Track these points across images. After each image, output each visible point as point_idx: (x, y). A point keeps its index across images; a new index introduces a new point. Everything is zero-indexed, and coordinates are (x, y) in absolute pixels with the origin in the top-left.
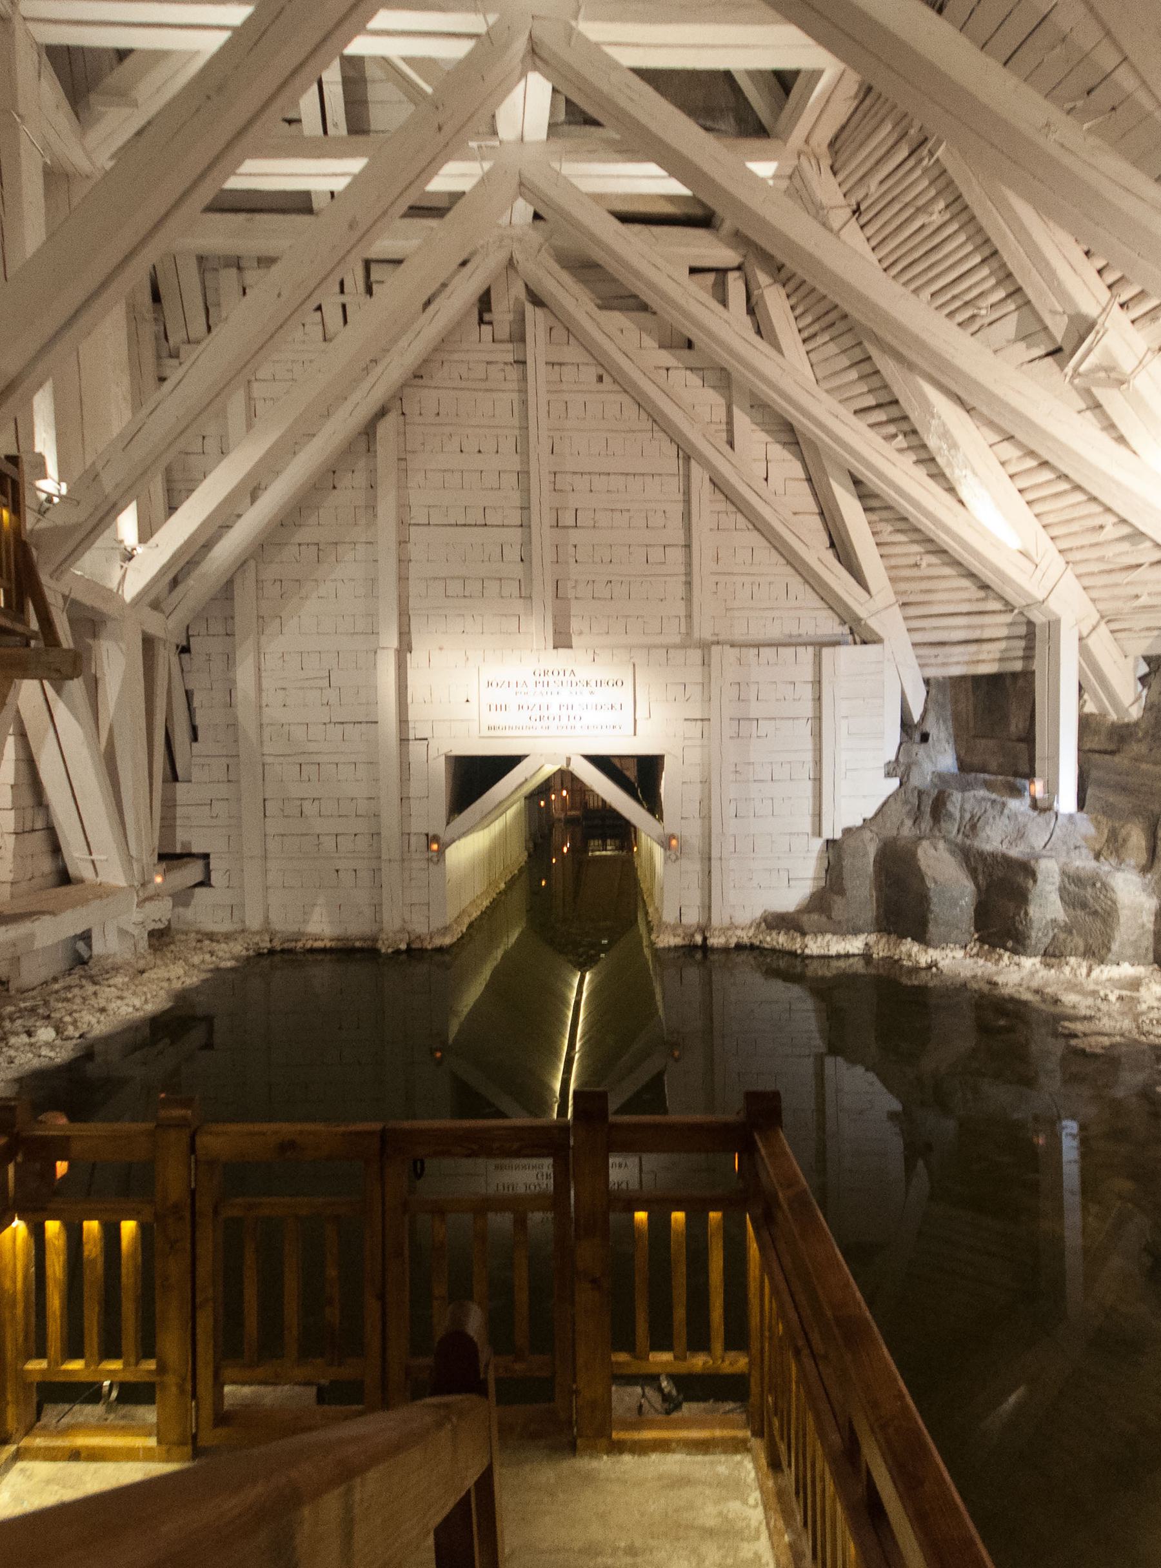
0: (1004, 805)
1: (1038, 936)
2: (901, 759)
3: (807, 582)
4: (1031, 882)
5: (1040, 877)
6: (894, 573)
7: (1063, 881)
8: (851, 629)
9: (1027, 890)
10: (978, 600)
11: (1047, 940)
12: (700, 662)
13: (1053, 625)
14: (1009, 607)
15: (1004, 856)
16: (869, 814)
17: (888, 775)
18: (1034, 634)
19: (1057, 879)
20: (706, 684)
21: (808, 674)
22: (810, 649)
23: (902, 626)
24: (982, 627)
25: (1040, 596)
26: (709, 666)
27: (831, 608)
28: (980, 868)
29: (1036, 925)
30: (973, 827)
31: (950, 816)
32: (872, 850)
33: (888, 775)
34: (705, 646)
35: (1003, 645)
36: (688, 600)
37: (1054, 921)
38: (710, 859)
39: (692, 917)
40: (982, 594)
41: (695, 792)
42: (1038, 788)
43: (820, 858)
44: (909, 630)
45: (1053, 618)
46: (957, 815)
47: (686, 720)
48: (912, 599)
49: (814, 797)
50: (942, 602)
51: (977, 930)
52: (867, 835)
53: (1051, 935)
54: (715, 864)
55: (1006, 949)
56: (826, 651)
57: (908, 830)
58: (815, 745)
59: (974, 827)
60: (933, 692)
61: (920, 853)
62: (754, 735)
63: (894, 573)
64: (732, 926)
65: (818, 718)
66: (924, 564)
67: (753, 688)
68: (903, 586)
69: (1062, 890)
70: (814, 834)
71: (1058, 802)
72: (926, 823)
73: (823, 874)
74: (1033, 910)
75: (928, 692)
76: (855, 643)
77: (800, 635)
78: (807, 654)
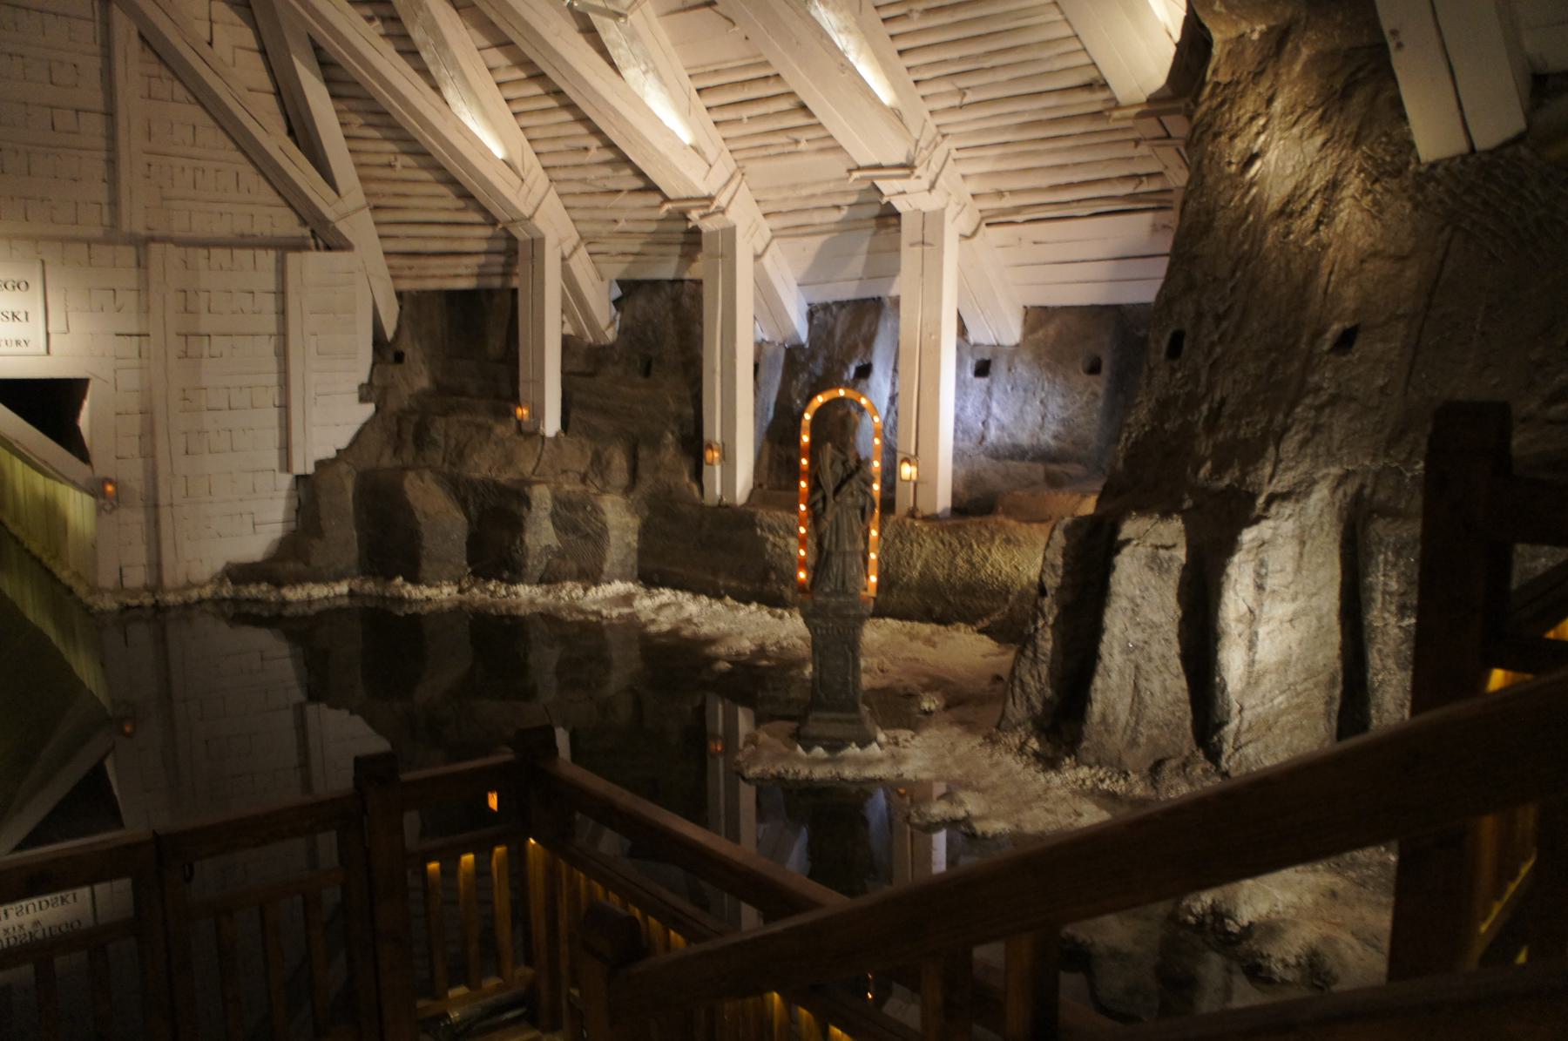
0: (490, 429)
1: (534, 564)
2: (375, 382)
3: (262, 173)
4: (525, 509)
5: (534, 503)
6: (366, 171)
7: (554, 506)
8: (313, 232)
9: (524, 518)
10: (458, 210)
11: (542, 567)
12: (133, 261)
13: (537, 243)
14: (493, 222)
15: (495, 483)
16: (343, 443)
17: (363, 399)
18: (516, 252)
19: (549, 504)
20: (143, 288)
21: (270, 282)
22: (272, 254)
23: (373, 232)
24: (462, 238)
25: (527, 212)
26: (146, 268)
27: (291, 206)
28: (470, 498)
29: (531, 553)
30: (461, 455)
31: (434, 443)
32: (349, 484)
33: (363, 399)
34: (142, 243)
35: (482, 259)
36: (112, 181)
37: (549, 547)
38: (156, 506)
39: (137, 577)
40: (461, 204)
41: (134, 424)
42: (522, 412)
43: (289, 497)
44: (381, 237)
45: (536, 236)
46: (442, 443)
47: (117, 335)
48: (383, 202)
49: (280, 426)
50: (417, 208)
51: (470, 563)
52: (343, 468)
53: (545, 560)
54: (164, 512)
55: (502, 580)
56: (293, 258)
57: (387, 461)
58: (279, 365)
59: (461, 455)
60: (406, 307)
61: (407, 484)
62: (206, 353)
63: (366, 171)
64: (190, 585)
65: (283, 334)
66: (398, 165)
67: (203, 296)
68: (374, 187)
69: (554, 516)
70: (281, 470)
71: (544, 426)
72: (408, 455)
73: (293, 515)
74: (529, 539)
75: (401, 307)
76: (317, 248)
77: (254, 236)
78: (268, 258)
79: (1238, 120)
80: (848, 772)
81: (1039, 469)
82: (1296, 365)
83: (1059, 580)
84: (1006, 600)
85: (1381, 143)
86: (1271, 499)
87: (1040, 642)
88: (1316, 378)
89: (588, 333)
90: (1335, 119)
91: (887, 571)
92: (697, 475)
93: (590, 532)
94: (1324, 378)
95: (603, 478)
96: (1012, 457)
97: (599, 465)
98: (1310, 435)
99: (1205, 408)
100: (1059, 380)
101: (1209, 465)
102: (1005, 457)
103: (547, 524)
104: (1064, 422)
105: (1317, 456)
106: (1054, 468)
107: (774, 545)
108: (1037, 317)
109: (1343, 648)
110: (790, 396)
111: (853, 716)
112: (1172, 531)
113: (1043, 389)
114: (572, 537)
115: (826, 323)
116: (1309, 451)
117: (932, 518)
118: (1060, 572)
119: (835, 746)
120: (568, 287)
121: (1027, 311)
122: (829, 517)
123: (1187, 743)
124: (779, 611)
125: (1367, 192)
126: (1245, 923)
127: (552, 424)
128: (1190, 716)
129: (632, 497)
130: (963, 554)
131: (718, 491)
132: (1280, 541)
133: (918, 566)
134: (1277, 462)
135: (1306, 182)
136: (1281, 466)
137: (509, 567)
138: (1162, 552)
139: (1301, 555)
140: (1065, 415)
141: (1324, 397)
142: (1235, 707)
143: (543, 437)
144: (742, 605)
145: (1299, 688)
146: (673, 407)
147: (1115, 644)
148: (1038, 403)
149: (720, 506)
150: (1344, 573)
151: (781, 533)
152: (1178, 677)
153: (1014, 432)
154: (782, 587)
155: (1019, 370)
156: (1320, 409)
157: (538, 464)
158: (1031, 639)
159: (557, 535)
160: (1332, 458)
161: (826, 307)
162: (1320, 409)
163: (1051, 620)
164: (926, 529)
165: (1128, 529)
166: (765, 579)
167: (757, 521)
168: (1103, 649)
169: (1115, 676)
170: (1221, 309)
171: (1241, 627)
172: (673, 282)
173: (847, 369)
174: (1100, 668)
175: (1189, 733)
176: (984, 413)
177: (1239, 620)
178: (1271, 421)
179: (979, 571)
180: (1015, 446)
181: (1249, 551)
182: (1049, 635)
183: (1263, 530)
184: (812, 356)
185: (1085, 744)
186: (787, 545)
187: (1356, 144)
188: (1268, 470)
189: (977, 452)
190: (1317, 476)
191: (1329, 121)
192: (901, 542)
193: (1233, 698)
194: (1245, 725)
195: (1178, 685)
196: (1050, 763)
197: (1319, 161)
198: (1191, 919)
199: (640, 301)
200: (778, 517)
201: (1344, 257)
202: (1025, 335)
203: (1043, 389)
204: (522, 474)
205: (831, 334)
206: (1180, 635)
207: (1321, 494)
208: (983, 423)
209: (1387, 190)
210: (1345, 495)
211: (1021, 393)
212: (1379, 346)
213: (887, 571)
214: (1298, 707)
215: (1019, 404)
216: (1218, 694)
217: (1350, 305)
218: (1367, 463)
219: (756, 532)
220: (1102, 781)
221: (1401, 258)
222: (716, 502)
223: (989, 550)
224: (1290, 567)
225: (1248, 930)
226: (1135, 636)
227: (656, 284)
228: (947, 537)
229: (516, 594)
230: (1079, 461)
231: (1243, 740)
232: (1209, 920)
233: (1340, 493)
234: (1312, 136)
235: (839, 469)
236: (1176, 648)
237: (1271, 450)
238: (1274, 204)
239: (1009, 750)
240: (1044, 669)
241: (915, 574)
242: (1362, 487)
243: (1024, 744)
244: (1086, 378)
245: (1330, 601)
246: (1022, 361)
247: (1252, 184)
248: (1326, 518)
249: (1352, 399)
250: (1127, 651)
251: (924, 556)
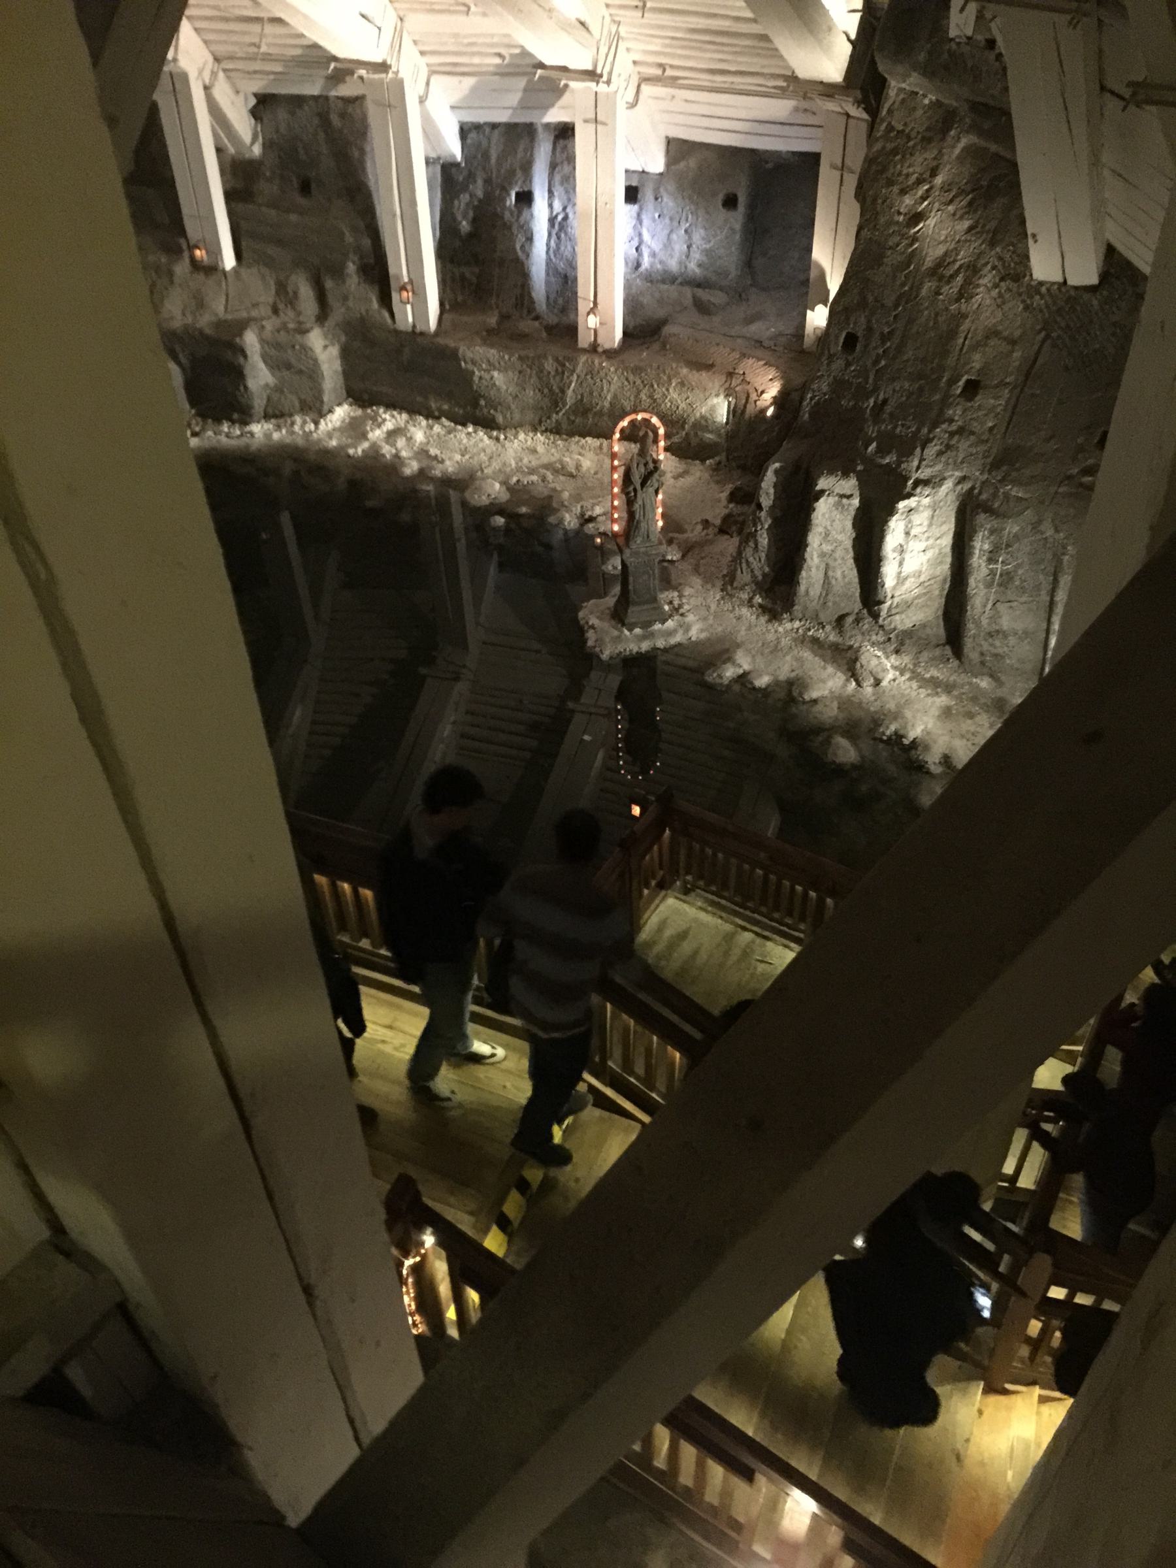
1: (259, 404)
4: (241, 360)
7: (263, 348)
37: (267, 385)
55: (233, 422)
69: (265, 358)
74: (252, 384)
79: (908, 175)
80: (661, 643)
81: (688, 292)
82: (937, 397)
83: (771, 502)
84: (683, 428)
85: (1009, 250)
86: (917, 483)
87: (760, 540)
88: (951, 412)
89: (229, 145)
90: (979, 212)
91: (582, 400)
92: (386, 299)
93: (303, 368)
94: (956, 412)
95: (294, 308)
96: (663, 282)
97: (285, 296)
98: (944, 450)
99: (872, 401)
100: (701, 212)
101: (874, 444)
102: (658, 281)
103: (262, 365)
104: (707, 253)
105: (948, 464)
106: (700, 292)
107: (481, 378)
108: (677, 149)
109: (952, 565)
110: (454, 219)
111: (655, 605)
112: (849, 485)
114: (286, 373)
115: (480, 144)
116: (943, 459)
117: (610, 354)
118: (772, 497)
119: (647, 625)
120: (217, 123)
121: (670, 142)
122: (640, 502)
123: (857, 605)
124: (495, 433)
125: (996, 286)
126: (911, 739)
127: (229, 260)
128: (859, 591)
129: (326, 324)
130: (645, 391)
131: (410, 319)
132: (921, 509)
133: (609, 398)
134: (921, 460)
135: (954, 253)
136: (924, 463)
137: (240, 413)
138: (845, 501)
139: (933, 516)
140: (708, 246)
141: (954, 427)
142: (890, 595)
143: (224, 272)
144: (460, 427)
145: (926, 584)
146: (349, 238)
147: (815, 553)
148: (683, 232)
149: (413, 332)
150: (956, 526)
151: (484, 366)
152: (852, 569)
153: (664, 258)
154: (492, 411)
155: (665, 199)
156: (952, 434)
157: (227, 301)
158: (753, 535)
159: (273, 375)
160: (957, 466)
161: (477, 127)
162: (952, 434)
163: (766, 526)
164: (612, 369)
165: (822, 483)
166: (476, 405)
167: (460, 356)
168: (807, 556)
169: (813, 570)
170: (886, 330)
171: (895, 555)
172: (315, 98)
173: (509, 195)
174: (805, 566)
175: (858, 599)
176: (636, 239)
177: (894, 551)
178: (919, 430)
179: (660, 405)
180: (665, 271)
181: (902, 514)
182: (765, 535)
183: (912, 502)
184: (471, 176)
185: (796, 607)
186: (492, 378)
187: (992, 244)
188: (916, 463)
189: (634, 276)
190: (947, 474)
191: (975, 211)
192: (592, 378)
193: (888, 591)
194: (895, 604)
195: (853, 575)
196: (773, 614)
197: (966, 241)
198: (885, 738)
199: (282, 114)
200: (478, 352)
201: (976, 330)
202: (668, 165)
203: (687, 220)
204: (216, 315)
205: (486, 155)
206: (854, 547)
207: (948, 485)
208: (637, 249)
209: (1009, 290)
210: (962, 489)
211: (667, 221)
212: (992, 401)
213: (582, 400)
214: (925, 594)
215: (666, 232)
216: (879, 587)
217: (977, 365)
218: (977, 474)
219: (460, 365)
220: (809, 630)
221: (1013, 342)
222: (410, 329)
223: (668, 390)
224: (926, 523)
225: (914, 741)
226: (827, 548)
227: (298, 101)
228: (631, 378)
229: (252, 434)
230: (721, 289)
231: (893, 612)
232: (894, 737)
233: (959, 487)
234: (961, 218)
235: (642, 469)
236: (851, 554)
237: (918, 450)
238: (929, 263)
239: (742, 604)
240: (763, 555)
241: (607, 404)
242: (973, 488)
243: (750, 600)
244: (722, 214)
245: (947, 541)
246: (666, 190)
247: (915, 239)
248: (949, 497)
249: (973, 433)
250: (823, 555)
251: (612, 390)
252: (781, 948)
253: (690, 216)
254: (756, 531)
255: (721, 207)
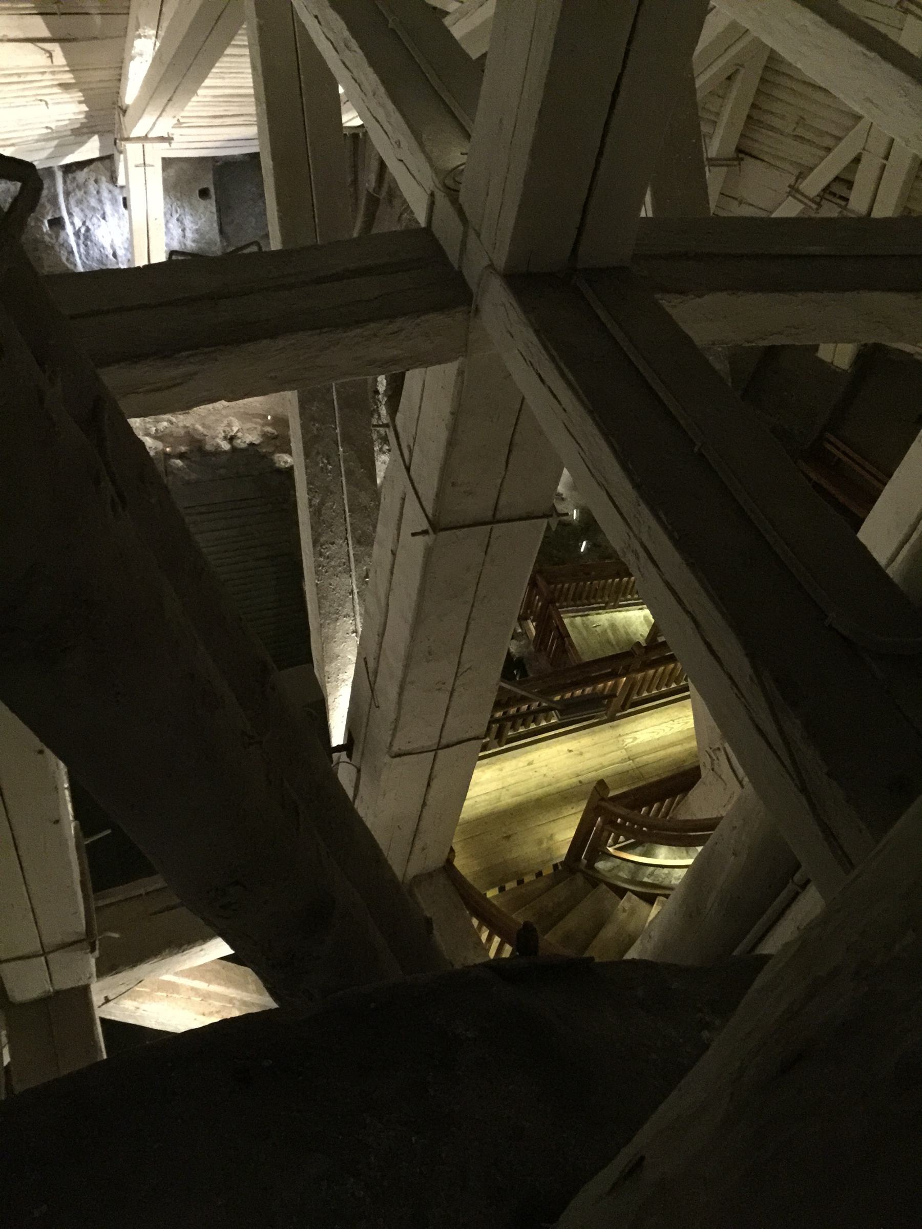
87: (381, 412)
113: (177, 212)
140: (197, 227)
158: (377, 411)
163: (384, 403)
182: (384, 408)
203: (177, 212)
244: (203, 203)
252: (595, 616)
253: (178, 210)
254: (378, 407)
255: (198, 197)
